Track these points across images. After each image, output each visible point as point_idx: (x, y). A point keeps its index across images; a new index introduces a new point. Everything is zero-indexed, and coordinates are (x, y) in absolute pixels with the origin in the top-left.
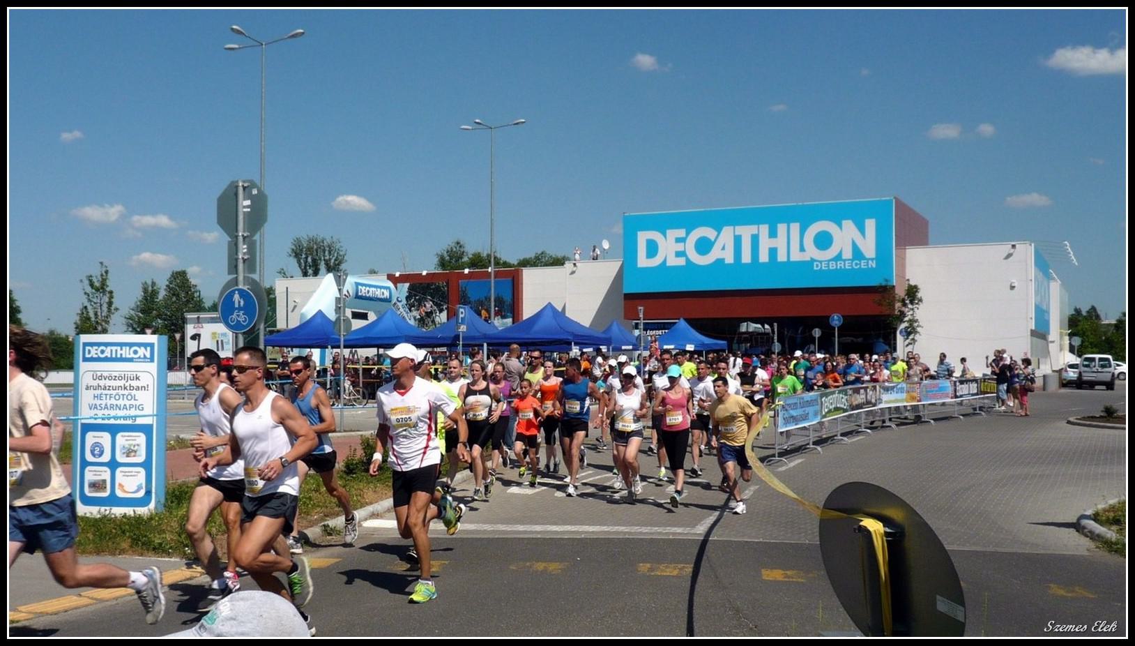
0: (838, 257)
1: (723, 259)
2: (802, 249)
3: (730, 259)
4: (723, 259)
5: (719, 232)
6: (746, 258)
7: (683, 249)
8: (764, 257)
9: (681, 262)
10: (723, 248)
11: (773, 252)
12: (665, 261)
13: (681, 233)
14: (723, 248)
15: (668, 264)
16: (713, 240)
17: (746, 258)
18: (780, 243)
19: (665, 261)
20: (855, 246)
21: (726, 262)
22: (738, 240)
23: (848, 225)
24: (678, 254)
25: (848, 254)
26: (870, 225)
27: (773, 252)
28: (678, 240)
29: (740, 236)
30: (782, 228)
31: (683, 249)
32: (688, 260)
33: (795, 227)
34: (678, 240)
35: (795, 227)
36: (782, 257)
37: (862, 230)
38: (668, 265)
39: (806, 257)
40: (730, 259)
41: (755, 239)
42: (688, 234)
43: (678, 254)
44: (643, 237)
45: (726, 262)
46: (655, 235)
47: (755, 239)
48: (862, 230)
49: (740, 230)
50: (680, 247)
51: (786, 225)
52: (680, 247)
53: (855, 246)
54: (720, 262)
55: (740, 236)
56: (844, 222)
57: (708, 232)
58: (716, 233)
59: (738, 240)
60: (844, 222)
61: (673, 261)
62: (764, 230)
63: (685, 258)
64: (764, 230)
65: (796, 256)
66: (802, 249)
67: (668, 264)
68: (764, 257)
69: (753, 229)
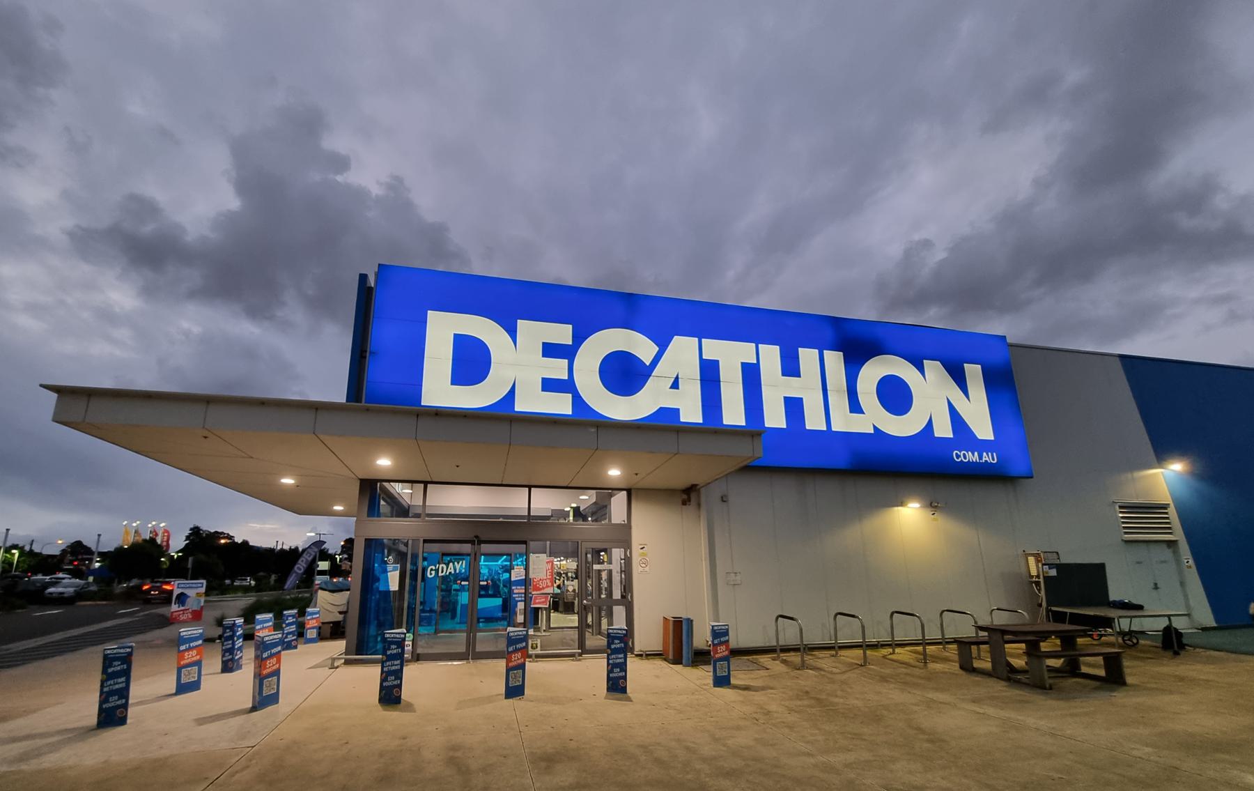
1: (676, 412)
2: (855, 407)
3: (692, 413)
4: (676, 412)
5: (663, 345)
6: (734, 413)
8: (775, 418)
9: (561, 405)
10: (675, 385)
11: (794, 407)
13: (562, 333)
14: (675, 385)
15: (520, 406)
17: (734, 413)
18: (806, 387)
24: (550, 385)
25: (944, 429)
27: (794, 407)
28: (550, 350)
30: (808, 357)
32: (578, 401)
34: (550, 350)
35: (835, 360)
36: (814, 421)
39: (860, 425)
40: (692, 413)
41: (751, 375)
42: (579, 338)
43: (550, 385)
47: (751, 375)
49: (715, 349)
52: (557, 368)
61: (532, 402)
62: (770, 356)
64: (770, 356)
65: (843, 422)
66: (855, 407)
67: (519, 407)
68: (775, 418)
69: (743, 352)
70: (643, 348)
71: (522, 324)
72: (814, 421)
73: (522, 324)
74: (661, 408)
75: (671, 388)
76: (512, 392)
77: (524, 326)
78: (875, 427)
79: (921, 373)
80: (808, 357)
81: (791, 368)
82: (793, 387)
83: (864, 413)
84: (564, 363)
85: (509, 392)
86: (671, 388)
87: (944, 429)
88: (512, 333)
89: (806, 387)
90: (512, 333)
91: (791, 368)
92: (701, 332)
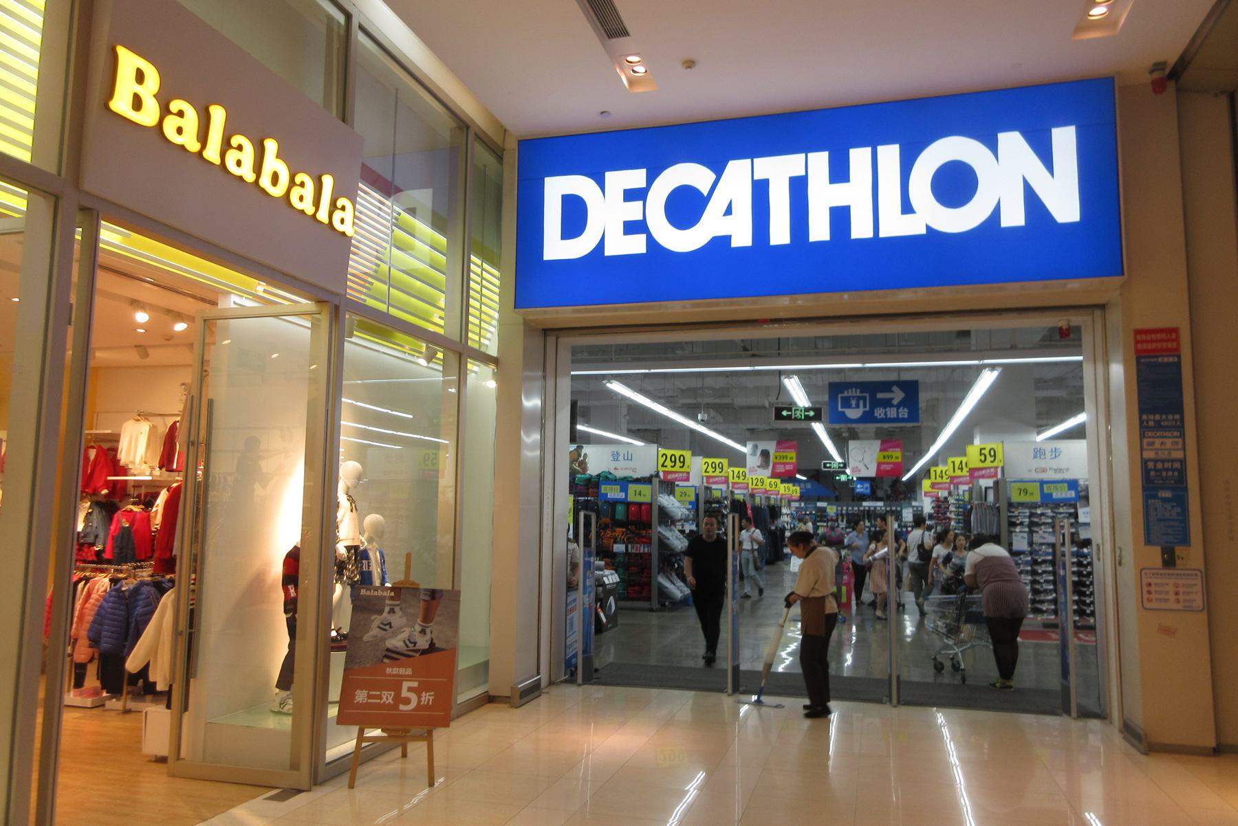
1: (728, 239)
2: (907, 208)
3: (742, 237)
4: (728, 239)
5: (719, 170)
6: (780, 234)
7: (641, 218)
8: (819, 230)
9: (636, 245)
10: (729, 211)
11: (840, 216)
12: (601, 245)
13: (636, 178)
14: (729, 211)
15: (609, 251)
16: (705, 194)
17: (780, 234)
18: (855, 194)
19: (601, 245)
20: (1032, 201)
21: (735, 243)
22: (760, 190)
23: (1012, 142)
24: (632, 228)
25: (1014, 217)
26: (1065, 139)
27: (840, 216)
28: (631, 195)
30: (859, 157)
31: (641, 218)
32: (651, 242)
33: (890, 154)
34: (631, 195)
35: (890, 154)
36: (861, 229)
37: (1045, 154)
38: (607, 254)
39: (912, 226)
40: (742, 237)
41: (799, 187)
42: (651, 179)
43: (632, 228)
44: (556, 188)
45: (735, 243)
46: (579, 185)
47: (799, 187)
48: (1045, 154)
50: (633, 211)
51: (868, 150)
52: (633, 211)
53: (1032, 201)
54: (721, 243)
56: (1002, 137)
57: (693, 174)
58: (713, 176)
59: (760, 190)
60: (1002, 137)
62: (820, 161)
63: (643, 237)
64: (820, 161)
65: (895, 225)
66: (907, 208)
67: (609, 251)
68: (819, 230)
72: (861, 229)
73: (610, 176)
74: (714, 238)
75: (725, 215)
77: (610, 176)
78: (928, 228)
79: (994, 154)
80: (859, 157)
81: (839, 173)
82: (840, 195)
86: (725, 215)
88: (601, 184)
89: (855, 194)
90: (601, 184)
91: (839, 173)
92: (752, 151)
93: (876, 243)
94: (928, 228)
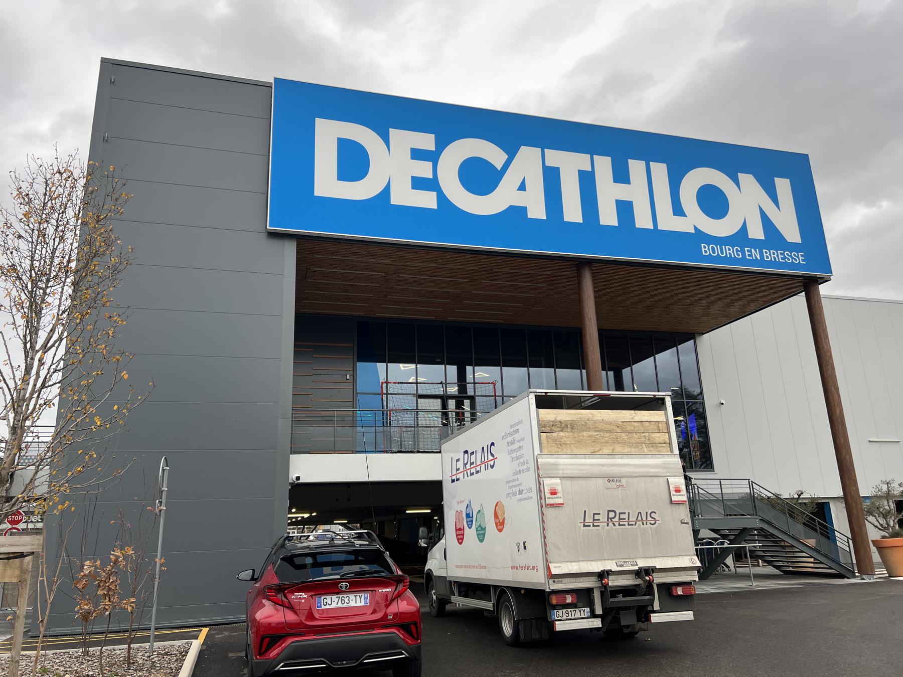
0: (741, 237)
1: (524, 210)
2: (678, 210)
3: (537, 211)
4: (524, 210)
5: (511, 154)
6: (573, 212)
8: (608, 217)
9: (427, 200)
10: (522, 187)
11: (625, 209)
12: (387, 190)
13: (427, 142)
14: (522, 187)
15: (396, 199)
17: (573, 212)
19: (386, 192)
21: (531, 215)
22: (551, 177)
24: (418, 183)
25: (756, 232)
26: (783, 186)
27: (625, 209)
29: (557, 170)
30: (636, 167)
32: (442, 198)
34: (417, 154)
35: (660, 171)
36: (643, 221)
40: (537, 211)
41: (587, 181)
42: (441, 145)
43: (418, 183)
45: (531, 215)
47: (587, 181)
49: (555, 158)
50: (424, 169)
52: (424, 169)
54: (517, 213)
55: (557, 170)
56: (741, 176)
58: (505, 157)
59: (551, 177)
62: (603, 166)
65: (669, 222)
66: (678, 210)
67: (396, 199)
68: (608, 217)
69: (581, 161)
70: (495, 155)
71: (393, 132)
76: (387, 188)
80: (636, 167)
82: (622, 192)
83: (686, 216)
84: (429, 165)
85: (386, 186)
87: (756, 232)
88: (386, 140)
90: (386, 140)
91: (621, 176)
93: (656, 235)
94: (695, 228)
